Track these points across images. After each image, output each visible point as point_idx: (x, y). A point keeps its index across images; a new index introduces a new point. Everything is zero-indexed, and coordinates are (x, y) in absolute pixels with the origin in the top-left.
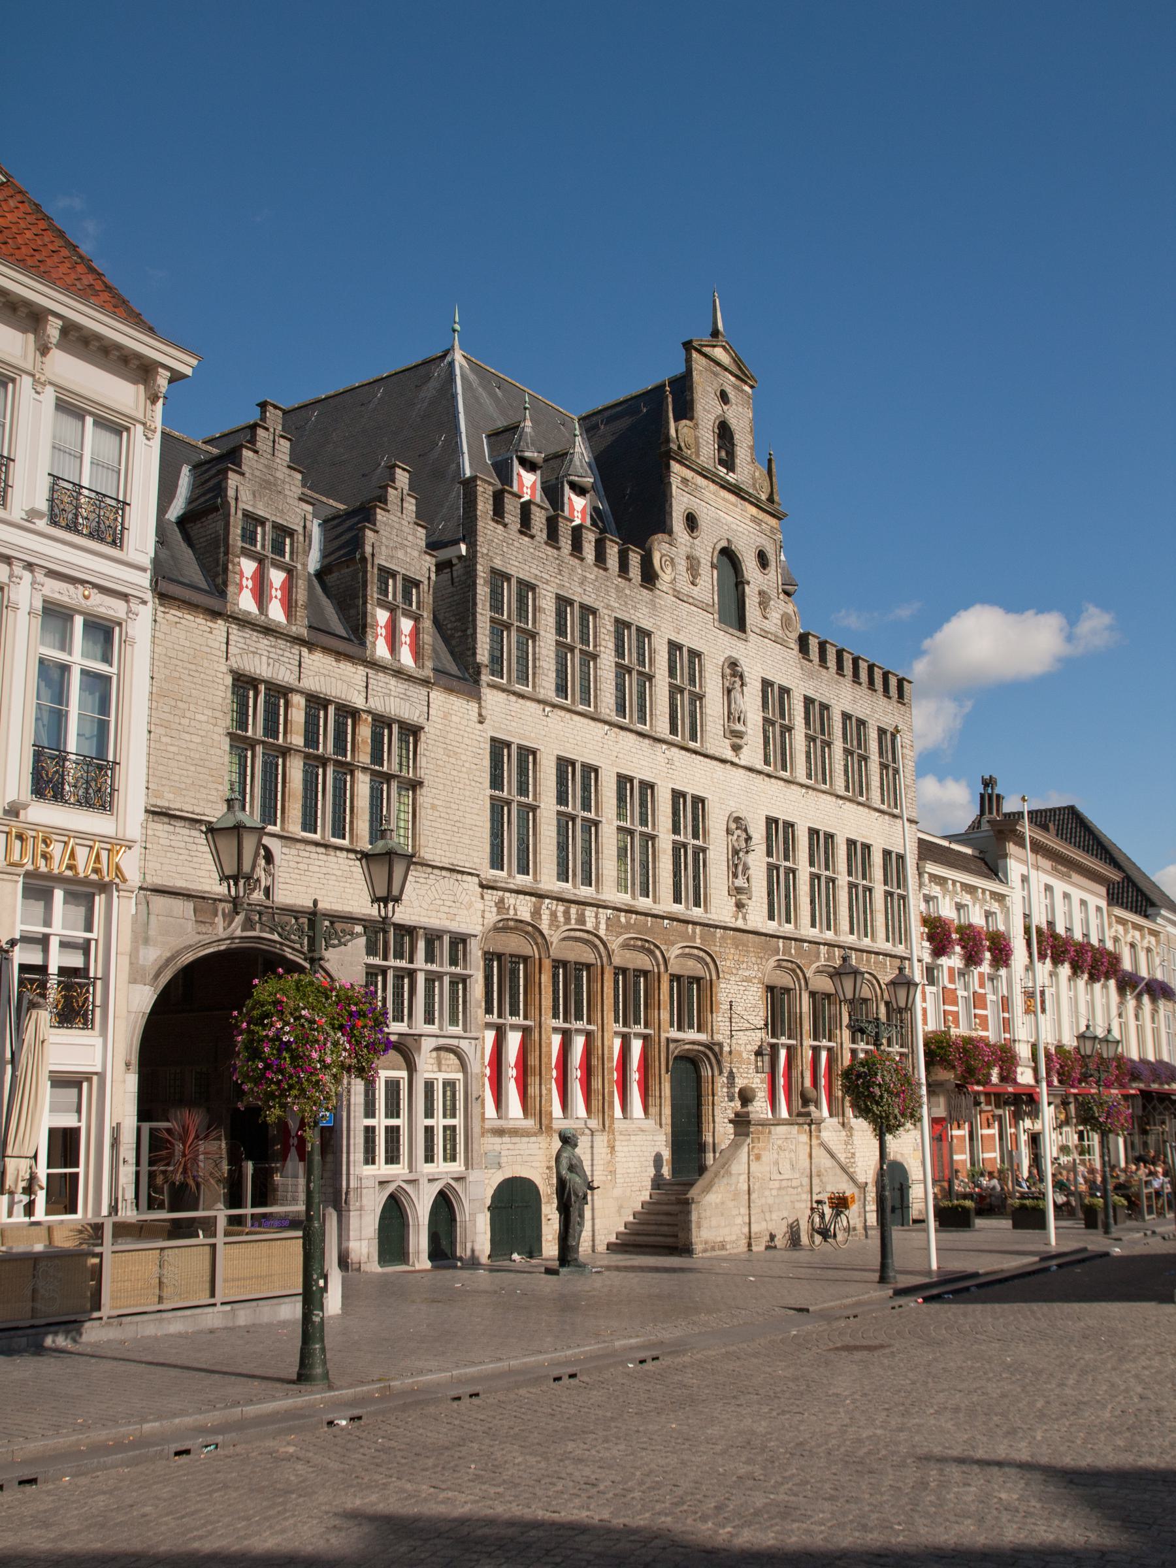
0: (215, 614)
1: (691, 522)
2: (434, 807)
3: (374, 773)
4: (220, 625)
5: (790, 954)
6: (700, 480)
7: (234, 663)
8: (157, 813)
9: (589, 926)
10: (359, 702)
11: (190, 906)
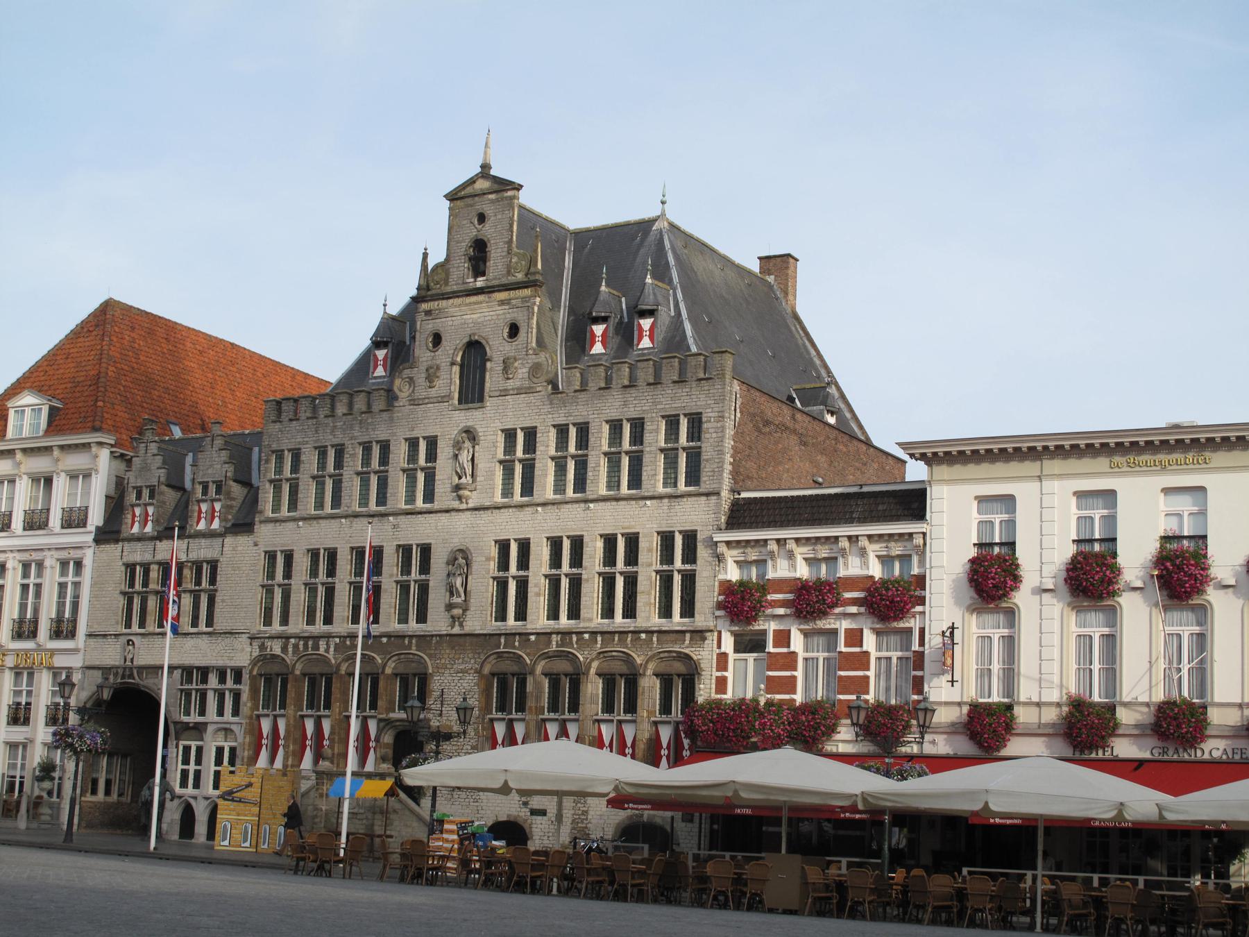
0: (117, 541)
2: (223, 601)
5: (514, 647)
6: (443, 303)
7: (125, 560)
8: (90, 635)
9: (322, 651)
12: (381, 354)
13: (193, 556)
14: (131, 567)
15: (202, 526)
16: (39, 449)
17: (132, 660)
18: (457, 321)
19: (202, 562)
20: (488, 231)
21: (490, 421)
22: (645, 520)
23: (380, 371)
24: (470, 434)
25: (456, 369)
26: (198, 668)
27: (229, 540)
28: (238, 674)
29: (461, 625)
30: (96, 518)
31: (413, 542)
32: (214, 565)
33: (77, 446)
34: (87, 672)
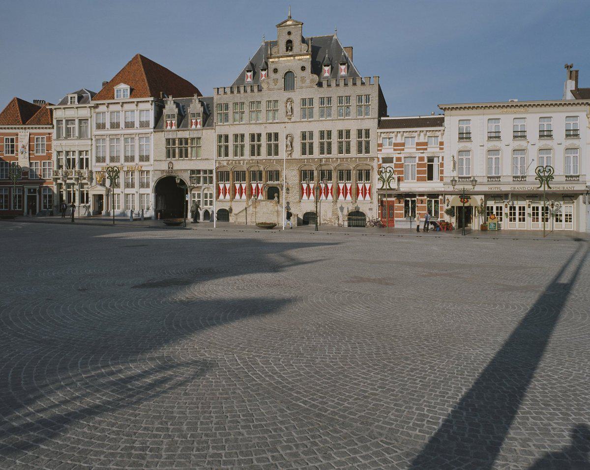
0: (162, 131)
3: (191, 147)
6: (277, 59)
7: (166, 137)
8: (155, 161)
10: (188, 137)
11: (160, 172)
12: (249, 74)
13: (192, 136)
14: (168, 140)
16: (129, 102)
18: (283, 65)
20: (292, 38)
21: (297, 96)
22: (353, 126)
23: (249, 80)
24: (289, 100)
25: (283, 79)
26: (196, 170)
27: (204, 131)
28: (211, 172)
29: (291, 156)
30: (152, 124)
31: (272, 132)
33: (143, 102)
34: (156, 172)
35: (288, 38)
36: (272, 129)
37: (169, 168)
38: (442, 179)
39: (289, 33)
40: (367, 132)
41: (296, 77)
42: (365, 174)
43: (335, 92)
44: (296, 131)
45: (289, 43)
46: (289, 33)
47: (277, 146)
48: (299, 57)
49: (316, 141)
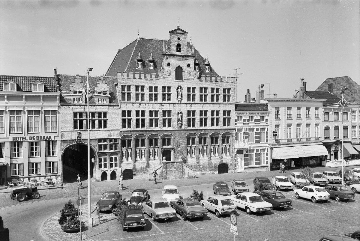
1: (169, 65)
4: (71, 107)
14: (75, 114)
15: (100, 103)
17: (80, 138)
19: (102, 112)
21: (185, 84)
25: (175, 72)
26: (102, 139)
27: (111, 108)
28: (116, 140)
32: (105, 114)
35: (177, 42)
36: (166, 108)
37: (78, 137)
38: (267, 141)
39: (179, 39)
40: (229, 112)
41: (184, 71)
42: (226, 138)
43: (209, 85)
44: (184, 109)
45: (179, 45)
46: (179, 39)
47: (169, 120)
48: (186, 58)
49: (198, 117)
